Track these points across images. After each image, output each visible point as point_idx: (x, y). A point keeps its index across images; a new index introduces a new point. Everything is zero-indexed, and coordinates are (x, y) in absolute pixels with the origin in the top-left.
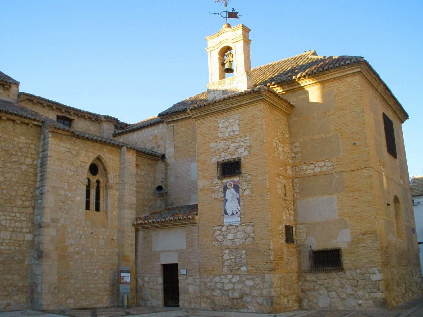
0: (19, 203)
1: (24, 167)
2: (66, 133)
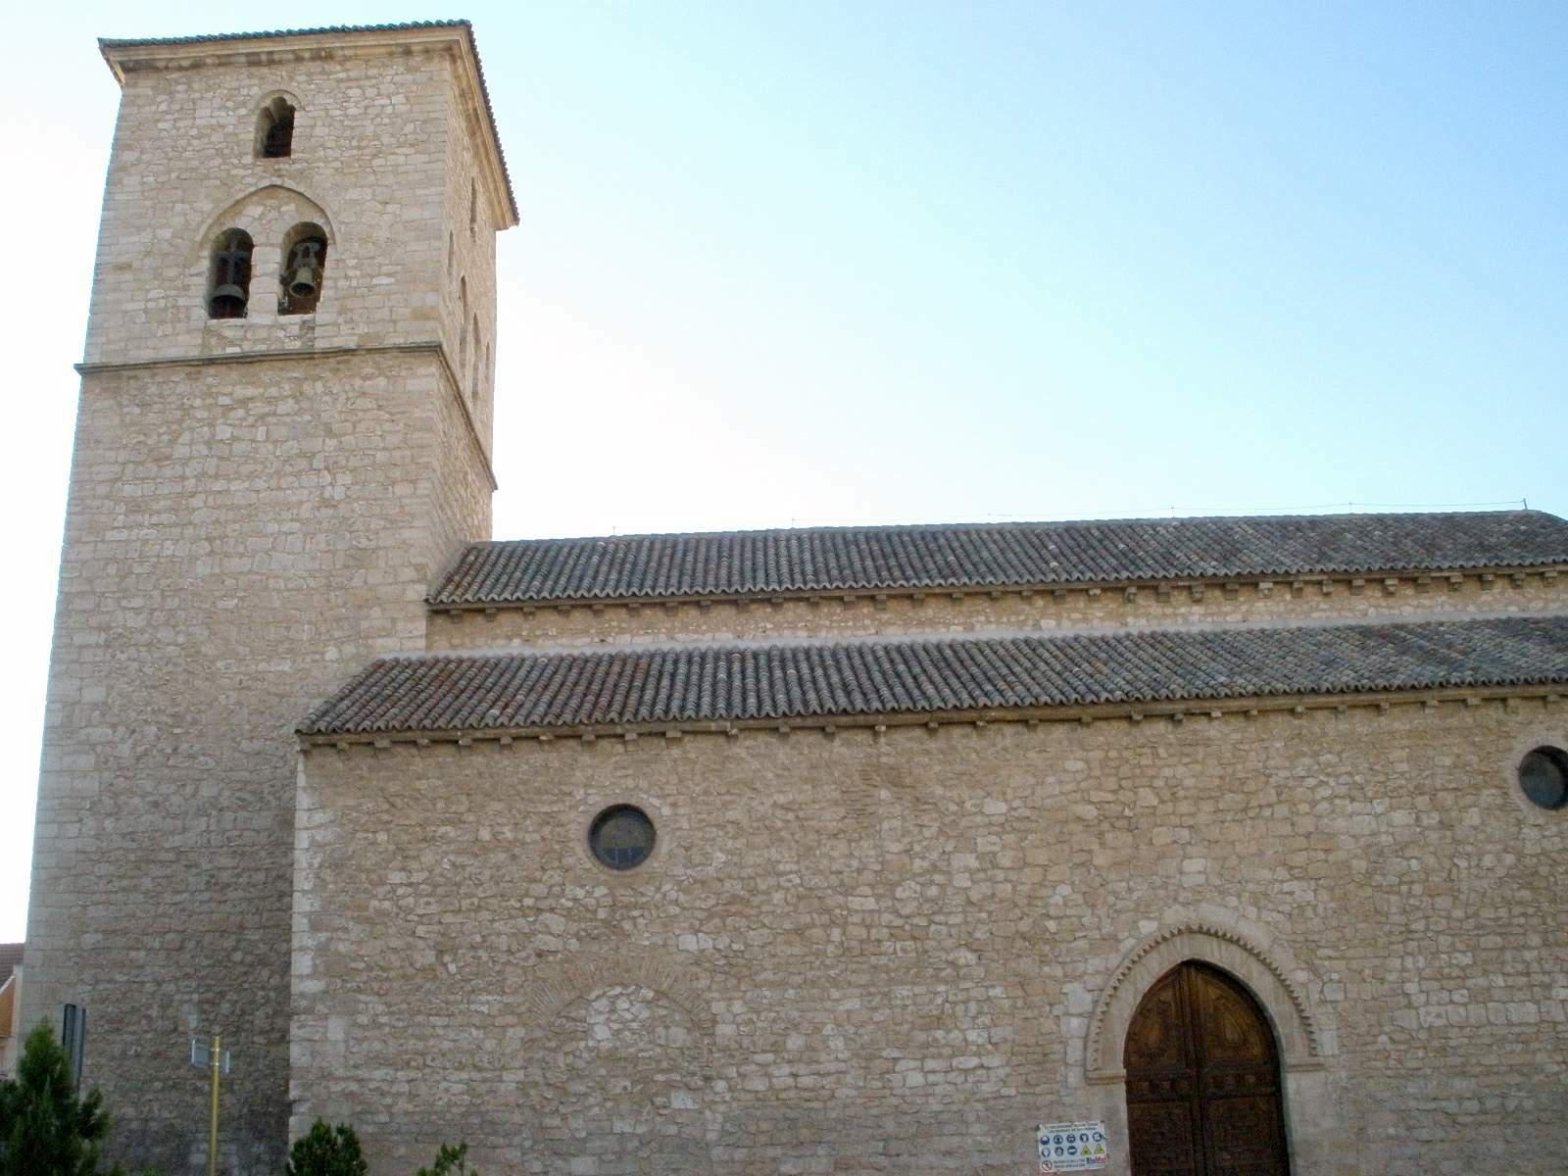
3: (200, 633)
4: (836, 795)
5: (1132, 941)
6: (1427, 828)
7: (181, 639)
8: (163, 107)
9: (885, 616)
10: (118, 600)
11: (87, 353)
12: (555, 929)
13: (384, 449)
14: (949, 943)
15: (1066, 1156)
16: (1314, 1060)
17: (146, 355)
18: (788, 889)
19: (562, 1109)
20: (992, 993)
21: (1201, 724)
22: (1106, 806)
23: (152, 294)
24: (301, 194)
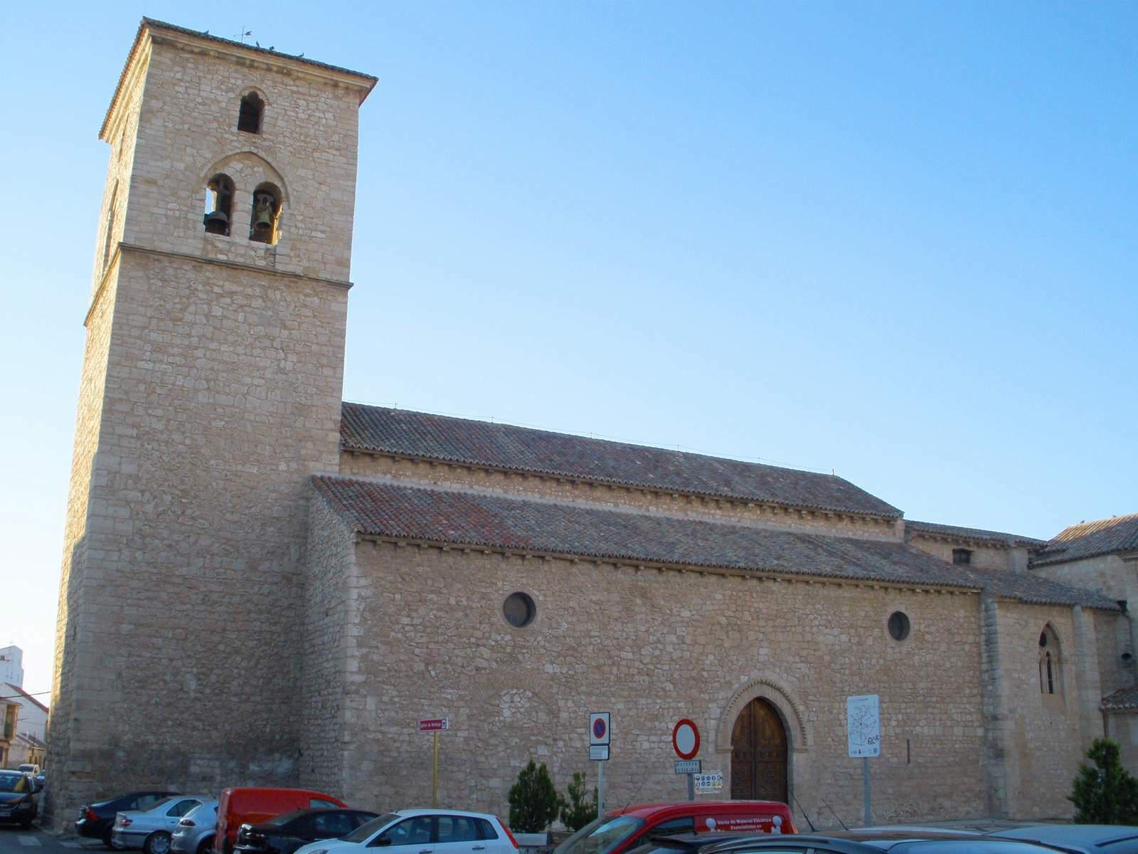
0: (967, 691)
1: (967, 647)
2: (1012, 601)
3: (201, 440)
4: (618, 599)
5: (737, 685)
6: (853, 644)
7: (188, 442)
8: (179, 76)
9: (577, 492)
10: (146, 409)
11: (125, 236)
12: (485, 656)
13: (317, 344)
14: (663, 679)
15: (706, 787)
16: (804, 747)
17: (165, 247)
18: (594, 645)
19: (486, 753)
20: (679, 705)
21: (770, 584)
23: (170, 206)
24: (269, 164)
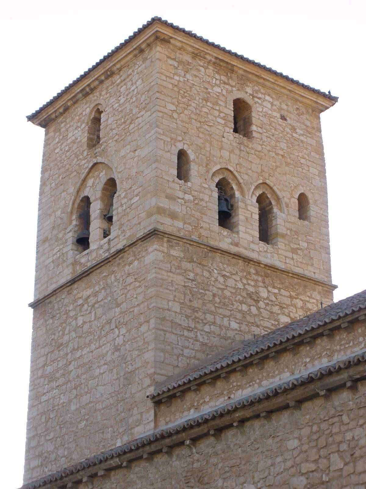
22: (311, 474)
